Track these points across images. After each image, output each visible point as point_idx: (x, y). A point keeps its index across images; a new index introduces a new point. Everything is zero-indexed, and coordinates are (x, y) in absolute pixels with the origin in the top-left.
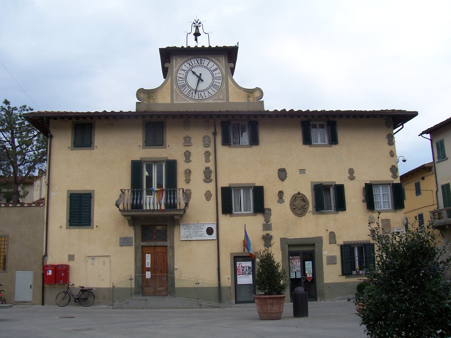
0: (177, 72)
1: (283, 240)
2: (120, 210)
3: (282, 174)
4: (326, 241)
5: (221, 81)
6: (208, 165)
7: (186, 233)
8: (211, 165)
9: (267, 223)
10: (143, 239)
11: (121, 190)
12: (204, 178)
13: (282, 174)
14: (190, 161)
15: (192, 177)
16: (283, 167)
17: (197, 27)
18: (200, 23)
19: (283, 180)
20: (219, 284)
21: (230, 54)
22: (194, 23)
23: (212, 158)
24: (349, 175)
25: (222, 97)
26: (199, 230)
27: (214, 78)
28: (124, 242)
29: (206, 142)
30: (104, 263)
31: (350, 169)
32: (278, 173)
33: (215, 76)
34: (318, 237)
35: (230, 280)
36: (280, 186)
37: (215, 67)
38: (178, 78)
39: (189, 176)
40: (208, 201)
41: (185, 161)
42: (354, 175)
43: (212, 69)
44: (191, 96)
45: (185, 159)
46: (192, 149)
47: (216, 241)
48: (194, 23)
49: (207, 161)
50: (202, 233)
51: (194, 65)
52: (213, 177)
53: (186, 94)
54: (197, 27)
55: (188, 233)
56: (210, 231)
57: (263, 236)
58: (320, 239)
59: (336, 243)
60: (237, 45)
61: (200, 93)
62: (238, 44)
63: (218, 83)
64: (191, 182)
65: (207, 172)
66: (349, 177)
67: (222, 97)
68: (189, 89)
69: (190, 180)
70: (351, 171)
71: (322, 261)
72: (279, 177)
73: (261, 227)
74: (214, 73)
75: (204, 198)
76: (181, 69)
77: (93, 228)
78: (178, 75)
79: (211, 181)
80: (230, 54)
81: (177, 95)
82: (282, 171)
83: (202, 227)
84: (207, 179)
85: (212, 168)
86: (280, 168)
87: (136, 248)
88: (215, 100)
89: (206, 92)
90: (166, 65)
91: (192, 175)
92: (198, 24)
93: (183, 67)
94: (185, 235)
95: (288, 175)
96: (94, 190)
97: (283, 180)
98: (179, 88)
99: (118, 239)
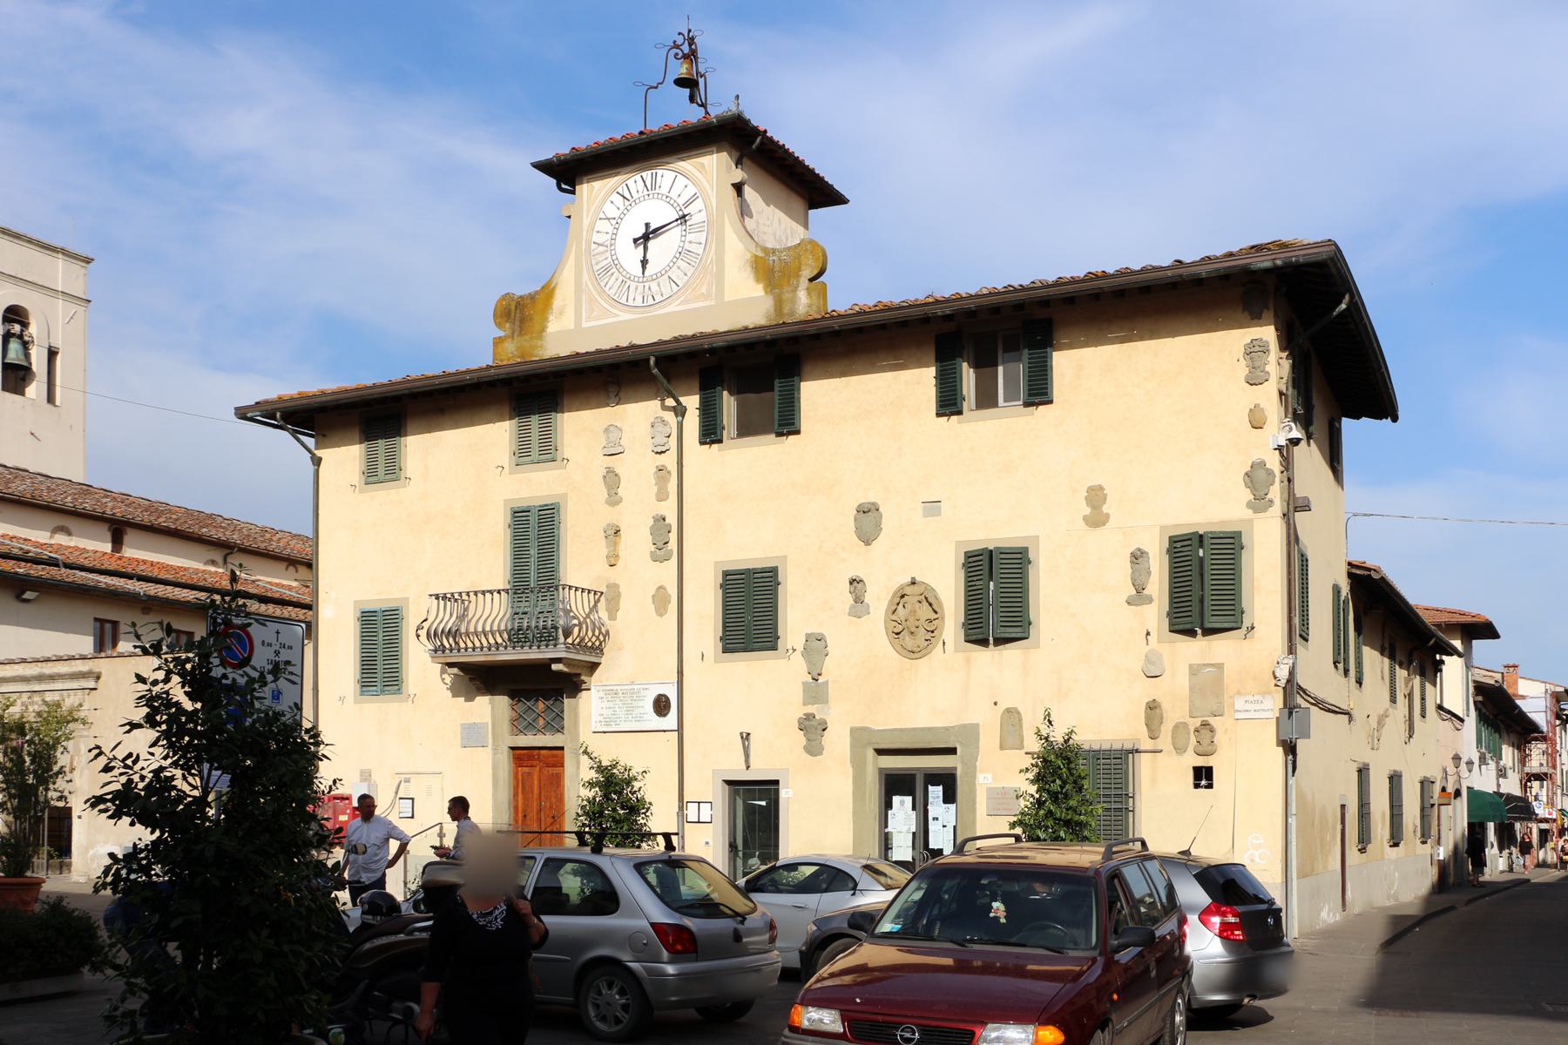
1: (859, 735)
3: (868, 519)
4: (989, 739)
7: (605, 712)
13: (868, 519)
14: (620, 500)
19: (868, 543)
22: (677, 47)
24: (1088, 511)
31: (1091, 489)
34: (965, 726)
36: (858, 561)
39: (615, 544)
42: (1105, 509)
48: (677, 47)
49: (662, 496)
52: (673, 545)
56: (661, 706)
58: (971, 732)
59: (1021, 747)
66: (1085, 519)
70: (1096, 496)
71: (974, 803)
84: (659, 552)
85: (672, 520)
88: (687, 301)
89: (664, 280)
95: (886, 523)
97: (868, 543)
98: (596, 278)
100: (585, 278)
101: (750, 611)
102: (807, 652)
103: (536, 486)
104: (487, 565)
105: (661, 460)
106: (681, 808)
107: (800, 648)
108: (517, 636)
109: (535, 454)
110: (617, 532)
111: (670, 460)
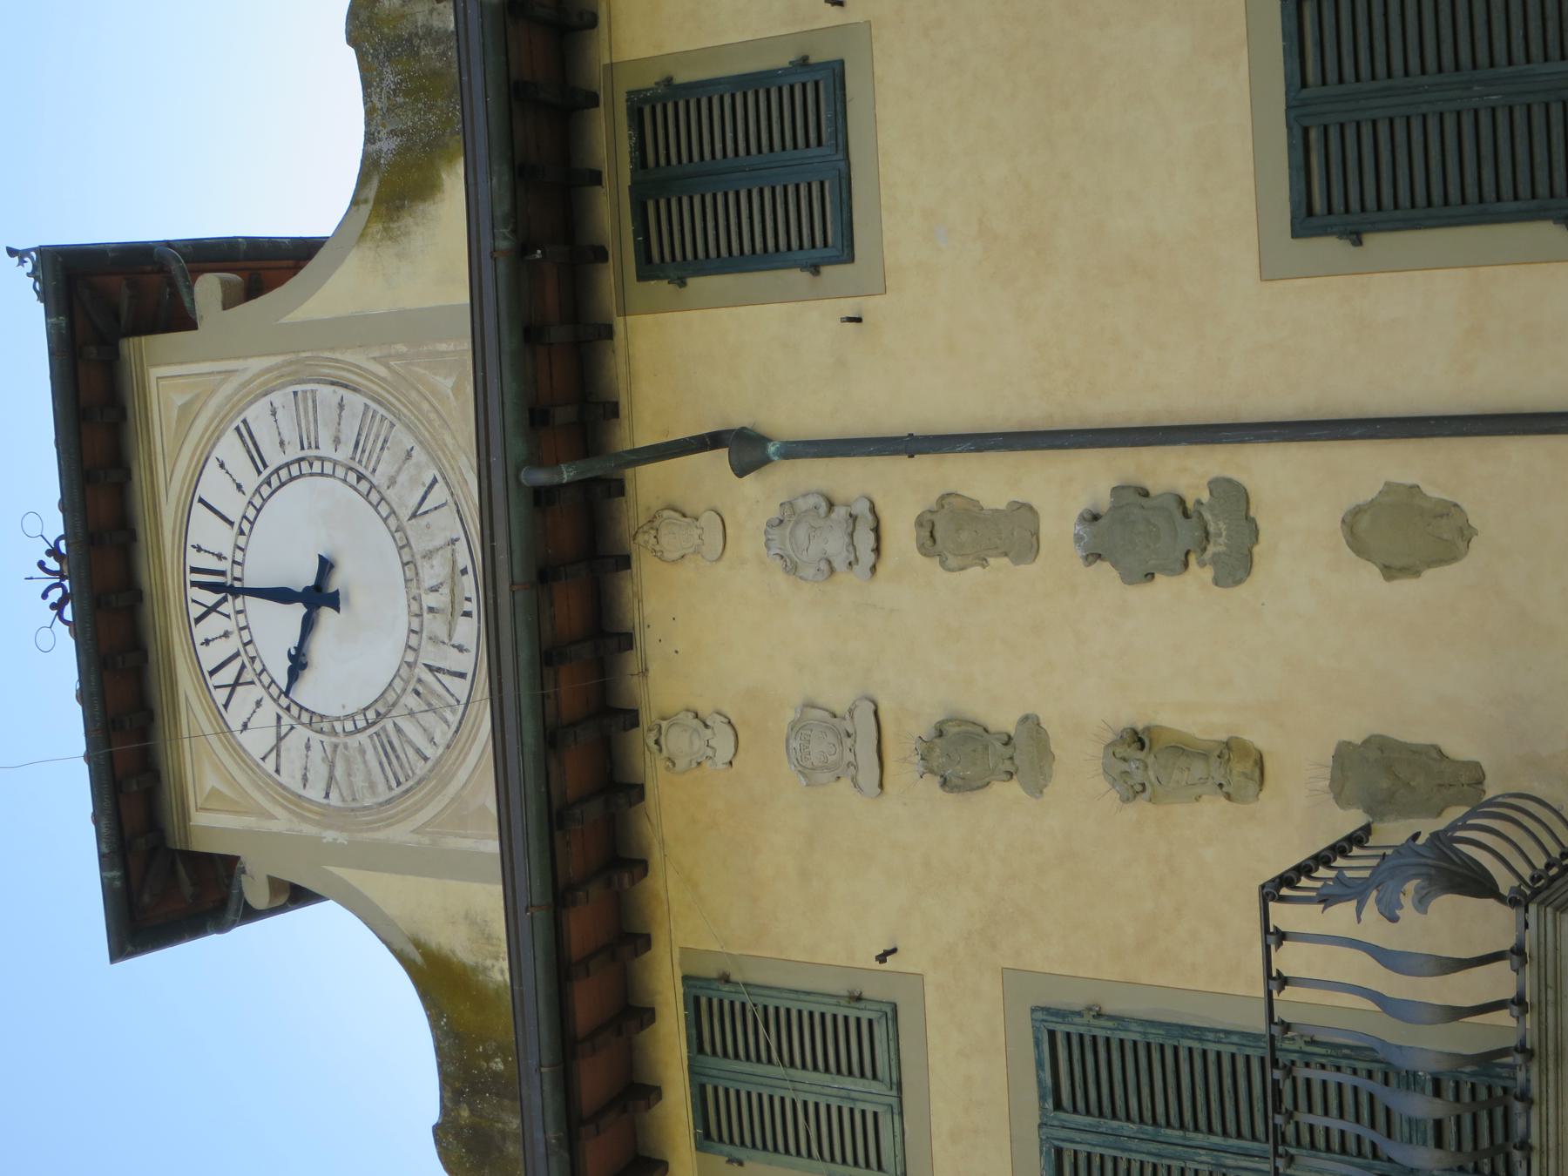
0: (295, 802)
5: (325, 391)
6: (1059, 528)
8: (1065, 489)
12: (1199, 575)
14: (1031, 722)
15: (1197, 716)
23: (989, 481)
29: (834, 544)
33: (294, 452)
37: (230, 448)
39: (1183, 749)
41: (1037, 788)
43: (251, 480)
45: (1013, 789)
49: (1015, 534)
51: (233, 645)
52: (1184, 472)
53: (442, 734)
61: (430, 600)
63: (338, 418)
64: (1257, 736)
65: (1137, 537)
68: (411, 701)
69: (1230, 750)
74: (274, 458)
75: (1435, 580)
76: (270, 765)
79: (1232, 495)
84: (1218, 536)
85: (1092, 477)
90: (257, 895)
91: (1168, 719)
93: (257, 742)
100: (400, 833)
109: (867, 1094)
110: (1138, 739)
111: (901, 490)
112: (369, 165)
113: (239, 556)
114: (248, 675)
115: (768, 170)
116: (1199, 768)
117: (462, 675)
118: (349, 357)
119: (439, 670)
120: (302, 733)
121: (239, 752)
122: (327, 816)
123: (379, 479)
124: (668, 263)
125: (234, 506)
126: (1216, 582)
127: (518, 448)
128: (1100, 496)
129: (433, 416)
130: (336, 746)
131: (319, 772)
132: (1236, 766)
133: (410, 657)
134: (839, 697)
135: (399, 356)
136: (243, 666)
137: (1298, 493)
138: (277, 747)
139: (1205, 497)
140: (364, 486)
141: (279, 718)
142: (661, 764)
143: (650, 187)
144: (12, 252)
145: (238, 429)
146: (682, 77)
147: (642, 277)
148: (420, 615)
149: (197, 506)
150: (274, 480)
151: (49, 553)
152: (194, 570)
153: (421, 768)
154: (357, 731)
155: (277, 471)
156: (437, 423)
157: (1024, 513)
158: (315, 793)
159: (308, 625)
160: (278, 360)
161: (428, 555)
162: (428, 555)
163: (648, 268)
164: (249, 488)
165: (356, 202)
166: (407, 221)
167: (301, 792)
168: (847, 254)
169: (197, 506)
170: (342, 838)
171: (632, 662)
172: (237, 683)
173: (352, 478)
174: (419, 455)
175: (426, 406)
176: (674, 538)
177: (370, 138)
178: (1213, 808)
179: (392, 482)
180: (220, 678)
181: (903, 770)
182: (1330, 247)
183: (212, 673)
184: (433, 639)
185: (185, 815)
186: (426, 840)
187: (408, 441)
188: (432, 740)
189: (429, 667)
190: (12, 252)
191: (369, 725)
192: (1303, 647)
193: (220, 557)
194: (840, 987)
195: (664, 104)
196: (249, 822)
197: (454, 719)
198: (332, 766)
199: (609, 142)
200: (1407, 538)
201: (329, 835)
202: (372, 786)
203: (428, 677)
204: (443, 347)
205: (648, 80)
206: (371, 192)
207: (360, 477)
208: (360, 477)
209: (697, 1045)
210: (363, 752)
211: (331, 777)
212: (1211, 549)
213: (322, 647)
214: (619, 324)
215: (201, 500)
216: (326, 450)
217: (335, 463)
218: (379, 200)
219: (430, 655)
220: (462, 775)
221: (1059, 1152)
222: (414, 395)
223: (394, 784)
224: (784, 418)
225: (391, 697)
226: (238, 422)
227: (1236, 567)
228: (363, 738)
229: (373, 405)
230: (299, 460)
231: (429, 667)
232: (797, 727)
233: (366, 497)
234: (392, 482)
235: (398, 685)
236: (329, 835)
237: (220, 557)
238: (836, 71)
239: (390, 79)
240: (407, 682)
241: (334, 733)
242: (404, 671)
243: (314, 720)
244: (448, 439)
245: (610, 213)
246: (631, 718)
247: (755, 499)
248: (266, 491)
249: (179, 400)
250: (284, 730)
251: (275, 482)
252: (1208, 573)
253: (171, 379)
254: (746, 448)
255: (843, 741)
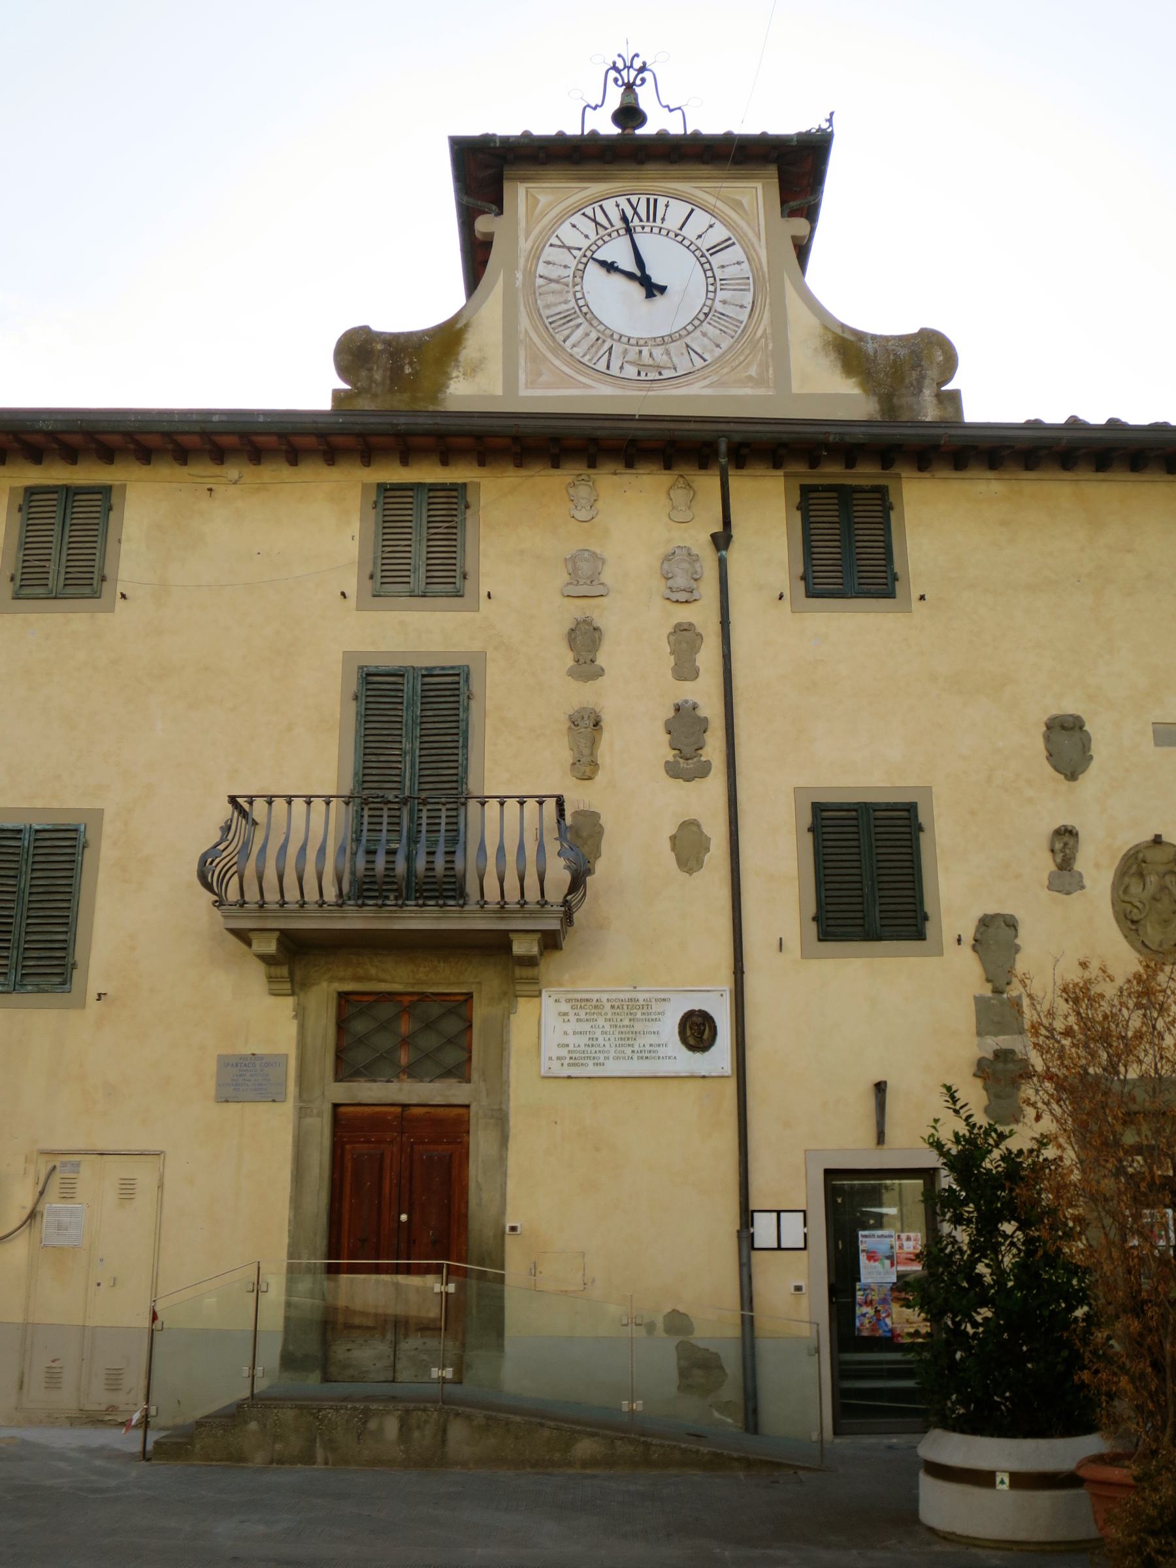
2: (219, 903)
3: (1067, 745)
5: (748, 298)
6: (689, 691)
7: (571, 1040)
8: (704, 693)
9: (997, 991)
10: (346, 1066)
11: (233, 800)
12: (670, 755)
13: (1067, 745)
14: (601, 672)
16: (1069, 706)
17: (629, 87)
18: (643, 69)
19: (1072, 776)
20: (748, 1323)
21: (794, 168)
22: (618, 71)
23: (708, 657)
25: (753, 371)
26: (638, 1027)
27: (713, 282)
28: (242, 1079)
29: (681, 581)
30: (127, 1190)
32: (1047, 739)
33: (719, 274)
35: (805, 1301)
37: (719, 233)
38: (539, 281)
39: (594, 743)
40: (690, 871)
41: (571, 673)
43: (705, 244)
44: (602, 366)
45: (570, 662)
46: (610, 617)
47: (731, 1087)
48: (614, 67)
49: (685, 670)
50: (652, 1039)
52: (714, 750)
53: (578, 352)
54: (629, 87)
55: (584, 1040)
56: (697, 1031)
57: (981, 1063)
60: (825, 125)
61: (645, 351)
62: (830, 121)
63: (736, 303)
64: (600, 777)
65: (684, 726)
67: (753, 371)
68: (594, 335)
69: (594, 765)
72: (1053, 756)
73: (965, 1017)
74: (716, 261)
75: (670, 858)
77: (82, 1005)
78: (542, 269)
79: (703, 771)
80: (794, 168)
81: (536, 358)
82: (1063, 728)
83: (656, 1007)
84: (685, 764)
85: (711, 708)
86: (1055, 711)
87: (302, 1112)
88: (720, 384)
90: (482, 224)
91: (606, 737)
92: (633, 73)
93: (566, 233)
94: (563, 1052)
95: (1099, 750)
96: (101, 812)
97: (1072, 776)
98: (547, 326)
99: (211, 1067)
100: (524, 322)
101: (868, 870)
102: (978, 944)
103: (417, 633)
104: (309, 759)
105: (684, 614)
106: (747, 1216)
107: (968, 938)
108: (366, 889)
110: (596, 724)
112: (860, 336)
113: (664, 232)
114: (602, 232)
115: (850, 557)
116: (586, 751)
117: (608, 368)
118: (767, 315)
119: (610, 353)
120: (573, 264)
121: (560, 220)
122: (530, 275)
123: (706, 327)
124: (807, 501)
125: (690, 232)
126: (667, 762)
127: (737, 438)
128: (703, 712)
129: (737, 362)
130: (567, 285)
131: (554, 272)
132: (586, 767)
133: (616, 337)
134: (607, 576)
135: (766, 345)
136: (606, 229)
137: (705, 800)
138: (563, 246)
139: (703, 759)
140: (702, 317)
141: (580, 249)
142: (569, 479)
143: (844, 495)
144: (832, 114)
145: (729, 239)
146: (893, 515)
147: (801, 486)
148: (637, 345)
149: (690, 207)
150: (704, 258)
151: (644, 63)
152: (656, 201)
153: (560, 338)
154: (577, 300)
155: (708, 262)
156: (734, 364)
157: (694, 674)
158: (542, 269)
159: (630, 276)
160: (765, 269)
161: (668, 353)
162: (668, 353)
163: (806, 490)
164: (699, 243)
165: (843, 326)
166: (833, 356)
167: (541, 260)
168: (810, 594)
169: (690, 207)
170: (519, 283)
171: (620, 468)
172: (597, 223)
173: (706, 310)
174: (718, 352)
175: (742, 358)
176: (680, 495)
177: (874, 337)
178: (567, 756)
179: (704, 334)
180: (598, 210)
181: (575, 610)
182: (808, 819)
183: (601, 206)
184: (625, 352)
185: (524, 179)
186: (522, 336)
187: (724, 346)
188: (574, 346)
189: (611, 347)
190: (832, 114)
191: (580, 308)
192: (640, 801)
193: (663, 219)
194: (469, 567)
195: (882, 503)
196: (522, 224)
197: (585, 360)
198: (557, 282)
199: (865, 474)
200: (688, 846)
201: (519, 275)
202: (548, 306)
203: (606, 347)
204: (771, 372)
205: (892, 498)
206: (847, 336)
207: (706, 315)
208: (706, 315)
209: (433, 487)
210: (566, 302)
211: (551, 280)
212: (681, 761)
213: (617, 280)
214: (780, 473)
215: (692, 210)
216: (721, 295)
217: (713, 300)
218: (843, 339)
219: (618, 349)
220: (557, 363)
221: (402, 676)
222: (747, 352)
223: (550, 320)
224: (735, 556)
225: (595, 323)
226: (734, 240)
227: (673, 771)
228: (573, 303)
229: (742, 326)
230: (714, 277)
231: (611, 347)
232: (594, 555)
233: (696, 318)
234: (704, 334)
235: (601, 328)
236: (519, 275)
237: (663, 219)
238: (891, 595)
239: (902, 352)
240: (603, 333)
241: (575, 285)
242: (608, 332)
243: (580, 272)
244: (726, 370)
245: (833, 473)
246: (592, 465)
247: (699, 538)
248: (698, 253)
249: (745, 201)
250: (575, 252)
251: (703, 260)
252: (671, 759)
253: (757, 194)
254: (722, 540)
255: (585, 576)
